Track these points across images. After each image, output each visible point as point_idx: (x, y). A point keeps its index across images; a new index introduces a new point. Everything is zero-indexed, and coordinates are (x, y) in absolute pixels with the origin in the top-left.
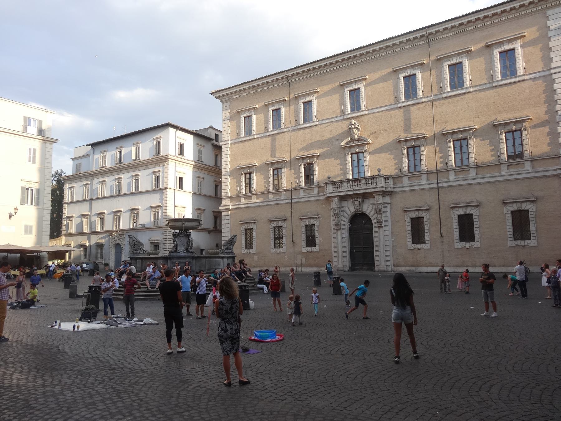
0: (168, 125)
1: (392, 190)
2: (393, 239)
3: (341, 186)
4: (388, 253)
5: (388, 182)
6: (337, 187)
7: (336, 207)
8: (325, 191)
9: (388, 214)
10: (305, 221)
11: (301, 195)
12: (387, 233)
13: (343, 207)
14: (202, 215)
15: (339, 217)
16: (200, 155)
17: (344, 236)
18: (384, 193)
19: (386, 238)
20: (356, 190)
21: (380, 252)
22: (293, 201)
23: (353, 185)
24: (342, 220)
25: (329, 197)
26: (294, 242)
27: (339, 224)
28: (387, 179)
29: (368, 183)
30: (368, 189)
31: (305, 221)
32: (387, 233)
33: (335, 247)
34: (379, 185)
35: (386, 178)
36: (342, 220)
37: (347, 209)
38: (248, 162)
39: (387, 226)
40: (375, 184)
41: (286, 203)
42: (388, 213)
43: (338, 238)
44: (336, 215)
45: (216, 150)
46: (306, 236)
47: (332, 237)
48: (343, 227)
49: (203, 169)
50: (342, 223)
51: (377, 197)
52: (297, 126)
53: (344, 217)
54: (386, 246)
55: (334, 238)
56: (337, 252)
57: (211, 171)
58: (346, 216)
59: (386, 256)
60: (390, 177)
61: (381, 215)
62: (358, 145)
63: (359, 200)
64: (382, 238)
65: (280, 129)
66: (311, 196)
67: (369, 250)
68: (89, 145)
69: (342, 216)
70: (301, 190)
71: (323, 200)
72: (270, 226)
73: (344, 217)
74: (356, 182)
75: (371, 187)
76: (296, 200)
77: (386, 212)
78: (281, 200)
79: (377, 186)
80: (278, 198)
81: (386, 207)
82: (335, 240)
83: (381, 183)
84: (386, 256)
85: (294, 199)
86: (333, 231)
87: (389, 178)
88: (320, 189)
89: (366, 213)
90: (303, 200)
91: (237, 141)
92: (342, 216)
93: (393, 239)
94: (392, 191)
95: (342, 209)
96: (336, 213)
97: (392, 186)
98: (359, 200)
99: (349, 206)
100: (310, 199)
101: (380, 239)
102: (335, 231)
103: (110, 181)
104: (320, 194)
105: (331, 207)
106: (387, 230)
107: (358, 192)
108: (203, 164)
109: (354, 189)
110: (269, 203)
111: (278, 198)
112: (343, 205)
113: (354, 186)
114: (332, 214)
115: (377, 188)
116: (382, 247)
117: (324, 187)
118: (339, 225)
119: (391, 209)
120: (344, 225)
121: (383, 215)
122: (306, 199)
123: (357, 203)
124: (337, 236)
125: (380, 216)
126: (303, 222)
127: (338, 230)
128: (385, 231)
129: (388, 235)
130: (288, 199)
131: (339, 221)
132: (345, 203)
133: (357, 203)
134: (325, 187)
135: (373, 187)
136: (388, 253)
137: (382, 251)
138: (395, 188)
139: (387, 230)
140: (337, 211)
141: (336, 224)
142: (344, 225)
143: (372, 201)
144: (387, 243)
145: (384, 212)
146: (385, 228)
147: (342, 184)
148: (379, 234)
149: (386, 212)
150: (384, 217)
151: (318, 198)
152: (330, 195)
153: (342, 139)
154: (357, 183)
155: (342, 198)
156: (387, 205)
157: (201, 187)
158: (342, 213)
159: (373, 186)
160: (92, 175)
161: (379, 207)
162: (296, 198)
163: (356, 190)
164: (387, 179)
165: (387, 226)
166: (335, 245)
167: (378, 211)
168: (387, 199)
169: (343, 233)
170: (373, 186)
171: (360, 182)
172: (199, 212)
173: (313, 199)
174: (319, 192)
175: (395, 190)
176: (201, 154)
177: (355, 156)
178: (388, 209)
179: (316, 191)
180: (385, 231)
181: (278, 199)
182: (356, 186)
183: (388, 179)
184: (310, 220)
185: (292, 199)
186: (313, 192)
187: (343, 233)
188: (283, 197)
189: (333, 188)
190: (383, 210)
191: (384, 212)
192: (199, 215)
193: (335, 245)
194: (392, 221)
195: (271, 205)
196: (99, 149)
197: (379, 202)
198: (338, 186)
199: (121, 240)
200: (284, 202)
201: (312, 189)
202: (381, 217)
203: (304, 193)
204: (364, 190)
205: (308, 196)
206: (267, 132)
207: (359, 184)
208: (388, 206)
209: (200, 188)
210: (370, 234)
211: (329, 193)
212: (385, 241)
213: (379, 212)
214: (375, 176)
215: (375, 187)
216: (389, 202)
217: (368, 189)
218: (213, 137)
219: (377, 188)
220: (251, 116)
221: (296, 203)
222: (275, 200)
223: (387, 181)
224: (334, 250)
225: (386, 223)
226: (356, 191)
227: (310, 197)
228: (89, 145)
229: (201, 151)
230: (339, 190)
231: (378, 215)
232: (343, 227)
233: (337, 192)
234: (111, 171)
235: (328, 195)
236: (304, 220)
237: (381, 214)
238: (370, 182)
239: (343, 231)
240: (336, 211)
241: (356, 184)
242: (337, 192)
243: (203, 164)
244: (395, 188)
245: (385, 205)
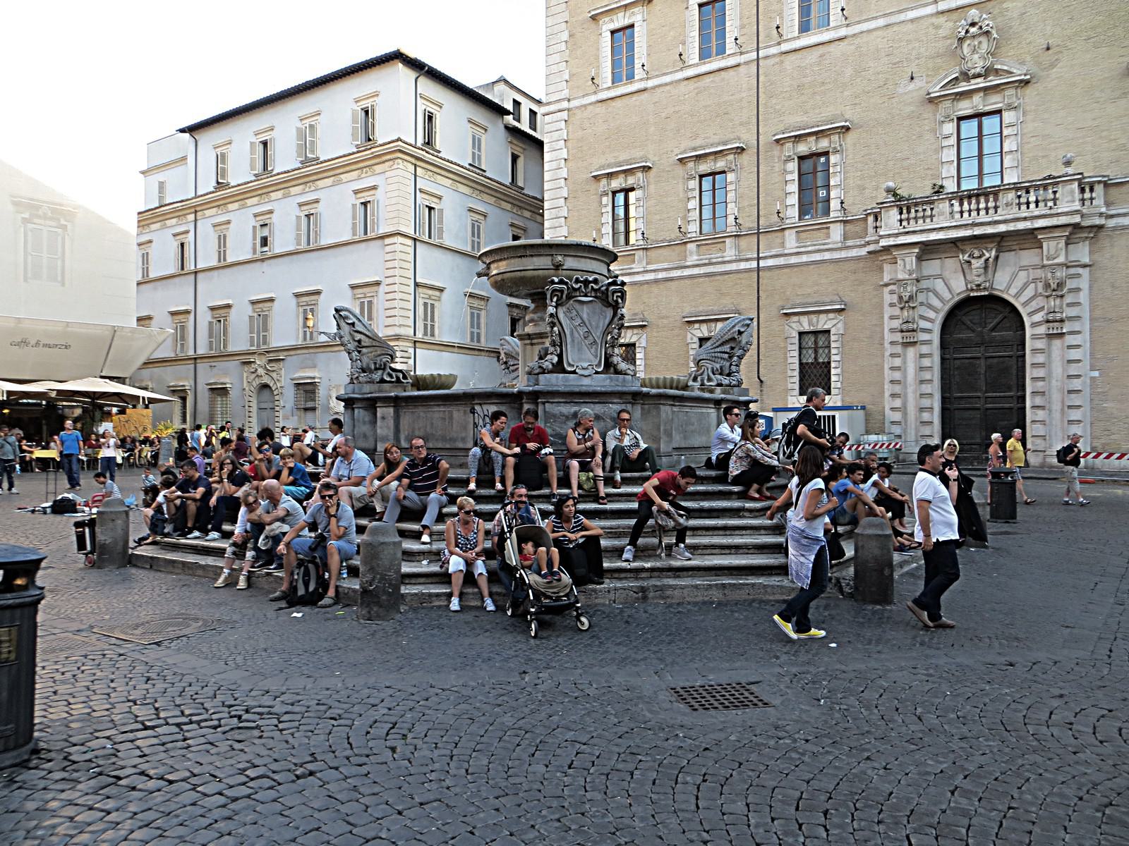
0: (397, 56)
1: (1101, 221)
2: (1096, 374)
3: (928, 213)
4: (1075, 415)
5: (1092, 199)
6: (916, 218)
7: (907, 277)
8: (871, 230)
9: (1083, 297)
10: (799, 322)
11: (788, 245)
12: (1074, 354)
13: (928, 278)
14: (483, 313)
15: (913, 308)
16: (477, 152)
17: (926, 362)
18: (1075, 232)
19: (1073, 370)
20: (982, 224)
21: (1050, 411)
22: (762, 264)
23: (970, 211)
24: (922, 317)
25: (887, 249)
26: (761, 382)
27: (915, 326)
28: (1087, 190)
29: (1023, 200)
30: (1025, 219)
31: (799, 322)
32: (1074, 354)
33: (893, 396)
34: (1063, 207)
35: (1085, 186)
36: (922, 317)
37: (939, 285)
38: (621, 159)
39: (1079, 332)
40: (1050, 204)
41: (738, 272)
42: (1081, 293)
43: (905, 370)
44: (906, 303)
45: (515, 142)
46: (801, 364)
47: (886, 367)
48: (924, 337)
49: (483, 189)
50: (924, 324)
51: (1053, 244)
52: (779, 44)
53: (930, 307)
54: (1070, 392)
55: (892, 369)
56: (903, 409)
57: (502, 197)
58: (936, 302)
59: (1070, 422)
60: (1099, 182)
61: (1062, 301)
62: (985, 89)
63: (987, 255)
64: (1058, 369)
65: (723, 58)
66: (822, 247)
67: (1007, 405)
68: (182, 131)
69: (922, 304)
70: (787, 232)
71: (859, 258)
72: (689, 336)
73: (930, 307)
74: (991, 199)
75: (1037, 213)
76: (770, 262)
77: (1078, 290)
78: (724, 262)
79: (1059, 211)
80: (715, 256)
81: (1079, 276)
82: (897, 375)
83: (1068, 202)
84: (1070, 422)
85: (765, 258)
86: (889, 350)
87: (1096, 187)
88: (849, 227)
89: (1005, 296)
90: (793, 260)
91: (589, 101)
92: (922, 304)
93: (1096, 374)
94: (1101, 227)
95: (924, 284)
96: (908, 294)
97: (1103, 210)
98: (987, 255)
99: (947, 274)
100: (817, 257)
101: (1050, 373)
102: (899, 349)
103: (242, 224)
104: (850, 243)
105: (886, 279)
106: (1078, 346)
107: (990, 230)
108: (485, 177)
109: (977, 221)
110: (687, 272)
111: (715, 256)
112: (925, 273)
113: (974, 214)
114: (888, 298)
115: (1058, 215)
116: (1056, 397)
117: (865, 220)
118: (913, 331)
119: (1092, 281)
120: (929, 331)
121: (1068, 299)
122: (804, 258)
123: (977, 264)
124: (905, 362)
125: (1058, 301)
126: (794, 325)
127: (907, 345)
128: (1070, 347)
129: (1079, 361)
130: (747, 260)
131: (914, 319)
132: (933, 267)
133: (978, 265)
134: (871, 219)
135: (1043, 212)
136: (1075, 415)
137: (1056, 406)
138: (1112, 216)
139: (1078, 346)
140: (911, 289)
141: (905, 327)
142: (929, 331)
143: (1028, 257)
144: (1076, 384)
145: (1070, 291)
146: (1070, 340)
147: (932, 209)
148: (1049, 356)
149: (1078, 290)
150: (1069, 305)
151: (843, 254)
152: (891, 242)
153: (927, 76)
154: (987, 201)
155: (928, 250)
156: (1080, 270)
157: (479, 237)
158: (921, 297)
159: (1042, 210)
160: (193, 210)
161: (1058, 274)
162: (771, 257)
163: (982, 224)
164: (1087, 190)
165: (1079, 332)
166: (897, 389)
167: (1054, 286)
168: (1082, 253)
169: (922, 356)
170: (1042, 210)
171: (996, 200)
172: (476, 303)
173: (827, 256)
174: (846, 237)
175: (1111, 223)
176: (479, 150)
177: (970, 128)
178: (1084, 283)
179: (836, 232)
180: (1070, 347)
181: (714, 260)
182: (983, 212)
183: (1092, 190)
184: (814, 317)
185: (758, 259)
186: (828, 236)
187: (922, 356)
188: (730, 253)
189: (901, 221)
190: (1070, 284)
191: (1070, 291)
192: (476, 312)
193: (897, 389)
194: (1091, 319)
195: (691, 277)
196: (210, 139)
197: (1056, 261)
198: (920, 214)
199: (274, 375)
200: (733, 267)
201: (825, 227)
202: (1061, 307)
203: (798, 240)
204: (1012, 224)
205: (810, 249)
206: (681, 69)
207: (991, 204)
208: (1085, 273)
209: (476, 239)
210: (1011, 357)
211: (889, 236)
212: (1069, 377)
213: (1056, 290)
214: (1055, 178)
215: (1049, 212)
216: (1086, 260)
217: (1025, 219)
218: (509, 107)
219: (1058, 215)
220: (632, 26)
221: (769, 268)
222: (707, 261)
223: (1087, 195)
224: (888, 403)
225: (1076, 326)
226: (984, 227)
227: (819, 251)
228: (182, 131)
229: (479, 140)
230: (920, 225)
231: (1051, 300)
232: (924, 337)
233: (914, 232)
234: (243, 195)
235: (883, 243)
236: (795, 318)
237: (1062, 296)
238: (1032, 198)
239: (925, 349)
240: (909, 289)
241: (973, 206)
242: (914, 232)
243: (485, 177)
244: (1112, 216)
245: (1072, 271)
